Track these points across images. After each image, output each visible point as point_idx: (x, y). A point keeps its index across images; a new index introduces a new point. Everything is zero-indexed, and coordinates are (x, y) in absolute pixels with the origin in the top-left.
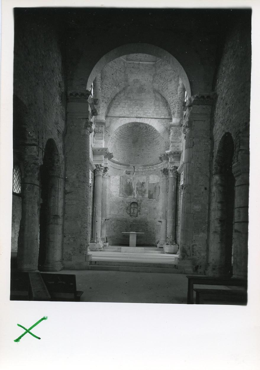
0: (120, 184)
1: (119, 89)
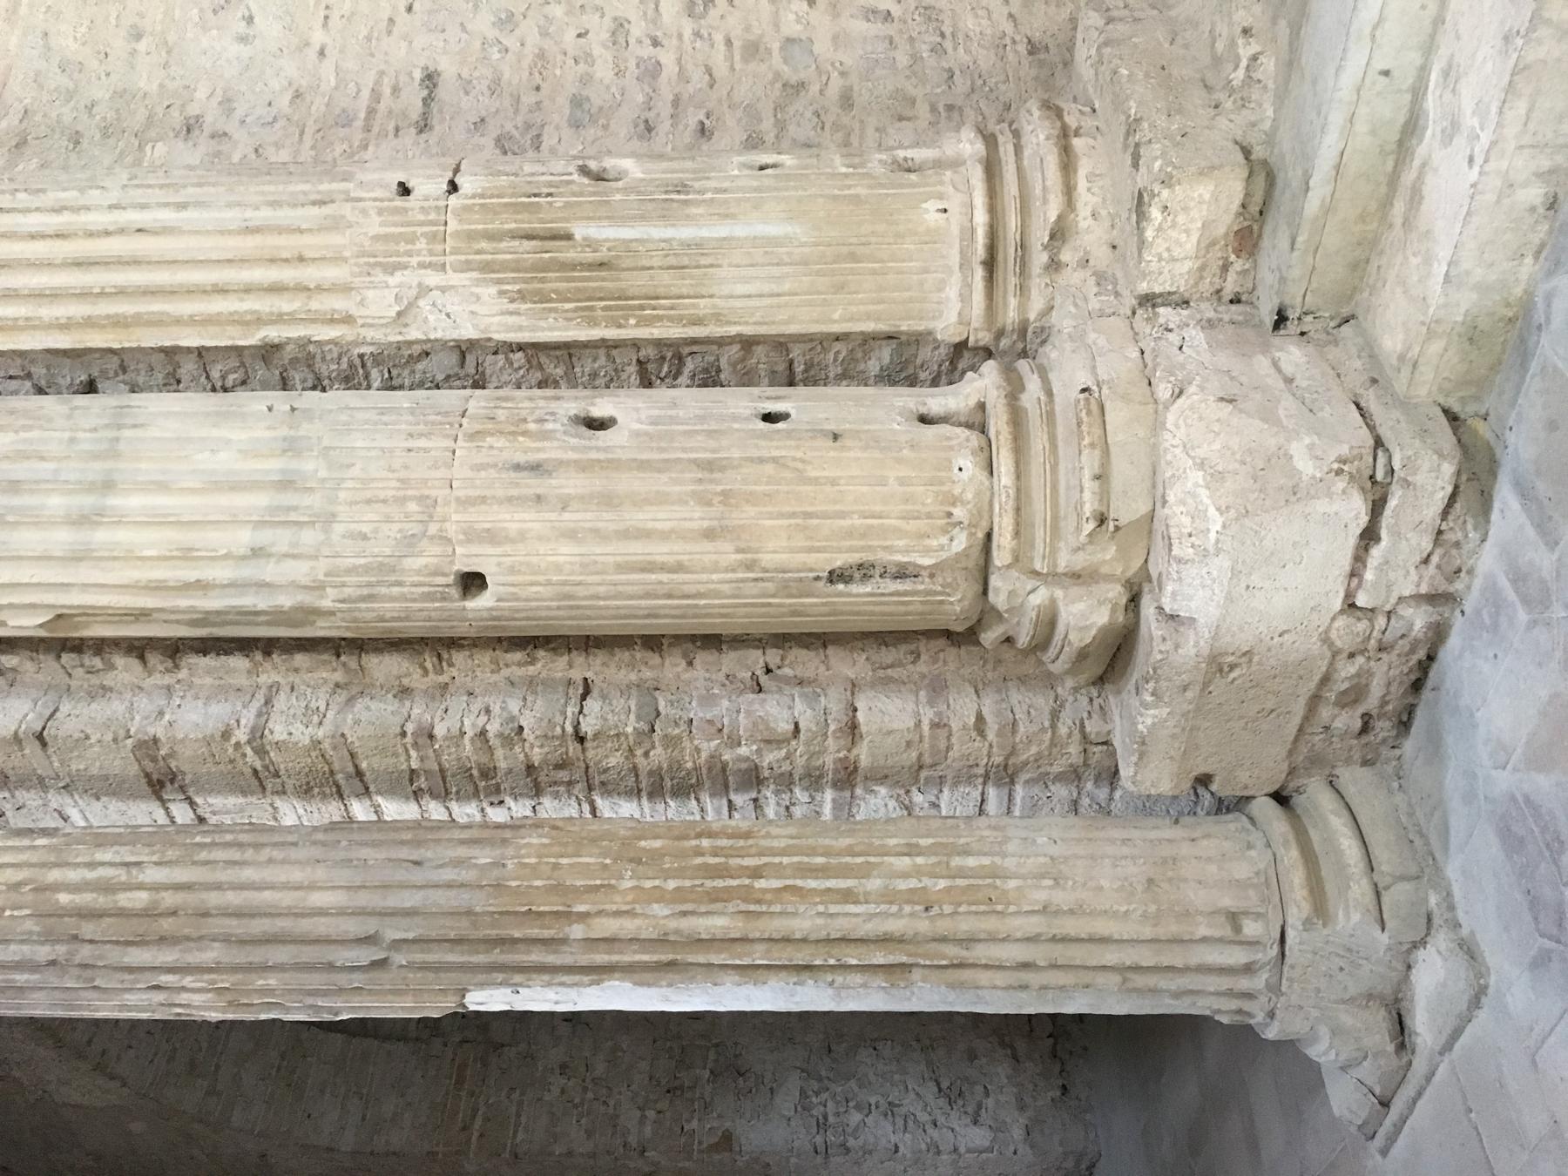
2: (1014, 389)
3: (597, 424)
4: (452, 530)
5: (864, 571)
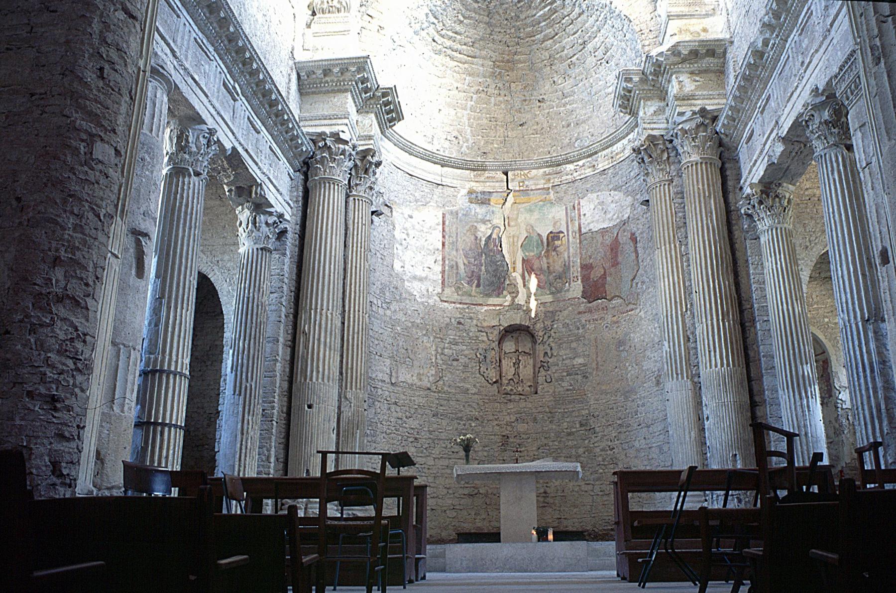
0: (443, 245)
4: (321, 405)
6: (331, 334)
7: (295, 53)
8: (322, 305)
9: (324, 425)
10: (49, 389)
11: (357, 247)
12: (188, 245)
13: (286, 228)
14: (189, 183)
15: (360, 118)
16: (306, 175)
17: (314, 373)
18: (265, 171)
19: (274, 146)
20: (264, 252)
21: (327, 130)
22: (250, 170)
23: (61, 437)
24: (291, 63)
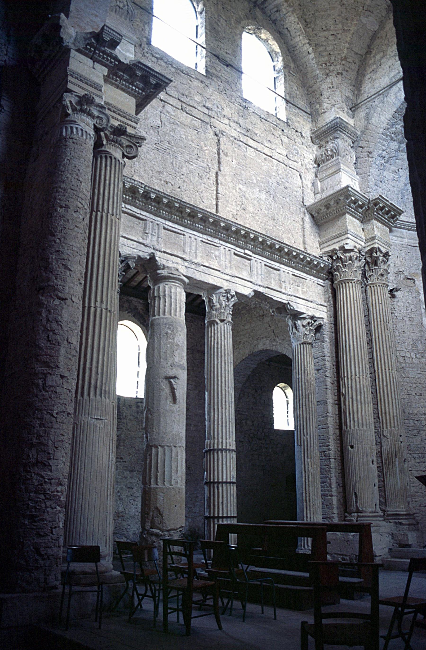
1: (371, 19)
2: (380, 516)
3: (373, 462)
4: (359, 445)
5: (356, 497)
6: (361, 393)
7: (305, 201)
8: (351, 373)
9: (363, 459)
10: (31, 512)
11: (377, 322)
12: (221, 368)
13: (320, 323)
14: (218, 329)
15: (365, 226)
16: (332, 281)
17: (352, 422)
18: (290, 293)
19: (297, 273)
20: (305, 345)
21: (337, 247)
22: (275, 298)
23: (38, 535)
24: (303, 209)
